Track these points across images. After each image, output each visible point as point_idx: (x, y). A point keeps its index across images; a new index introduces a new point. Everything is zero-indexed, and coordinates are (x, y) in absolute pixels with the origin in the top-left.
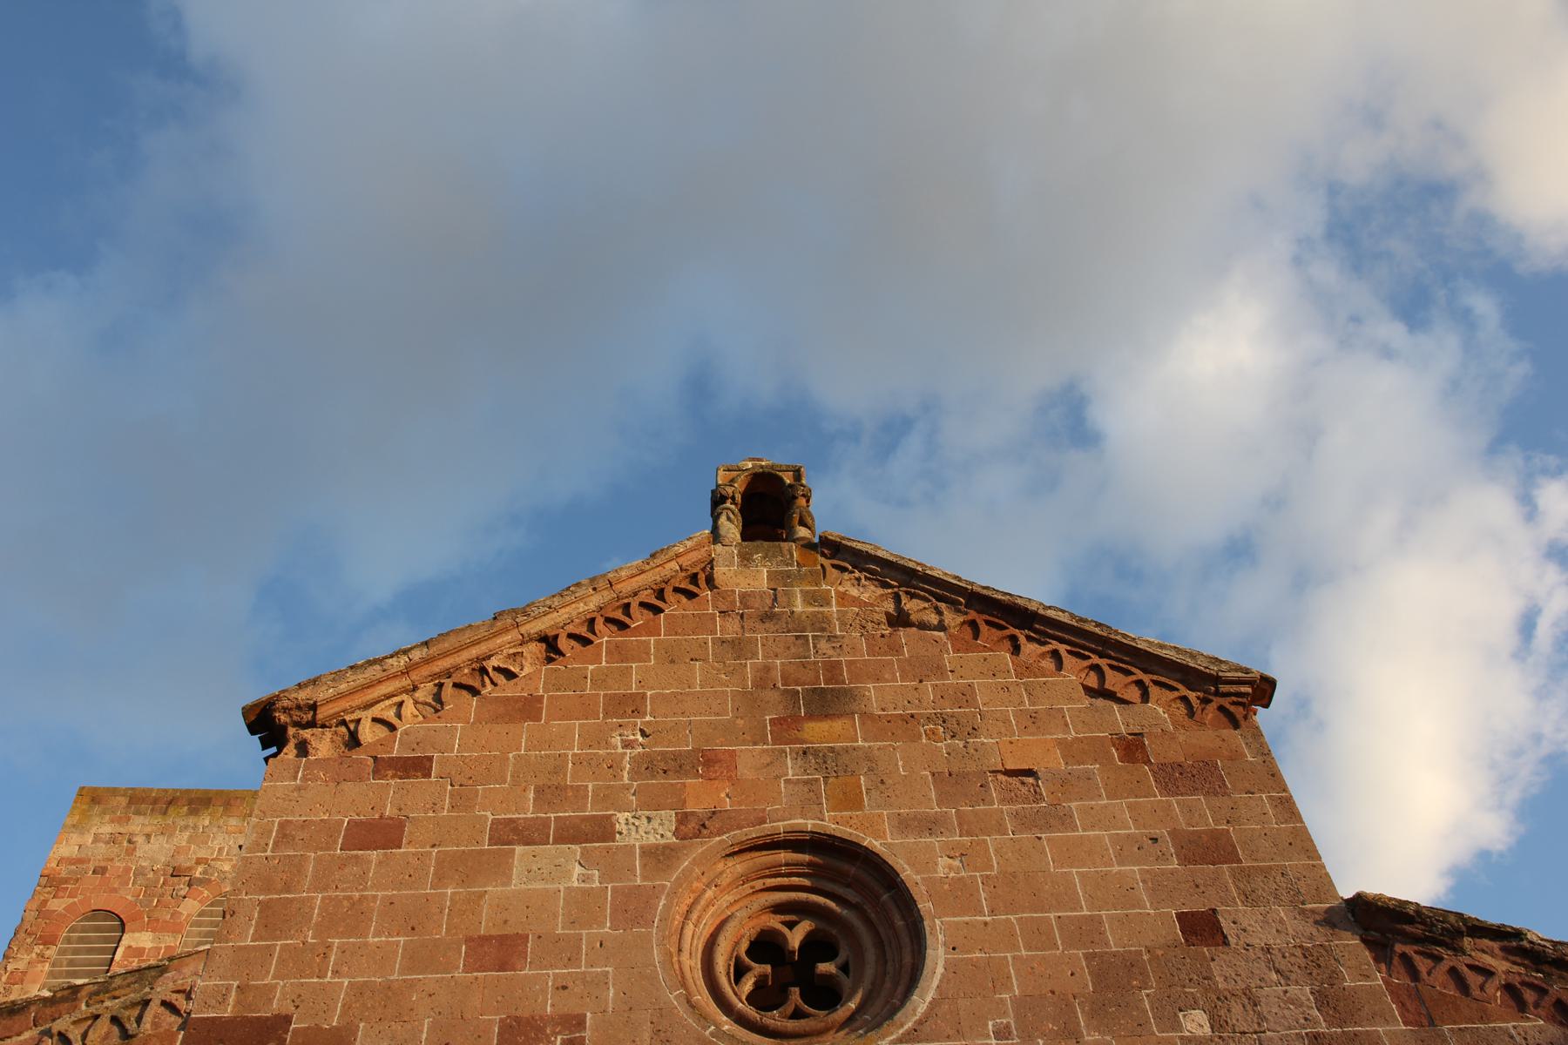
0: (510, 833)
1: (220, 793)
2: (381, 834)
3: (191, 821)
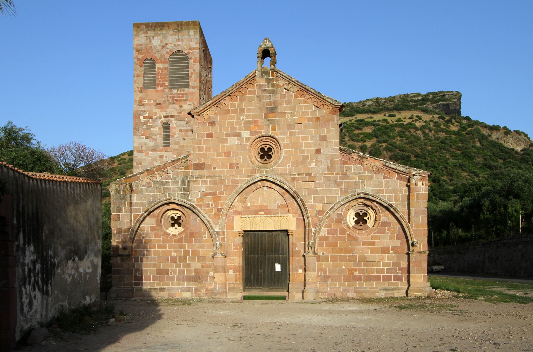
0: (228, 135)
1: (166, 23)
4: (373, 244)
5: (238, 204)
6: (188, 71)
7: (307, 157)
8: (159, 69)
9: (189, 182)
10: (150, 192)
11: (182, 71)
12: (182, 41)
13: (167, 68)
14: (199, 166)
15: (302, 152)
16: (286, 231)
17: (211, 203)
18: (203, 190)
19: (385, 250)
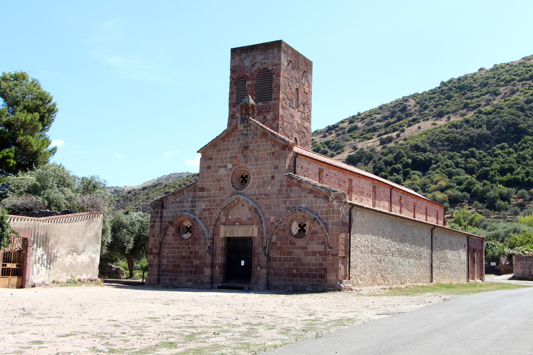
0: (220, 167)
2: (209, 167)
3: (252, 53)
4: (306, 248)
6: (272, 85)
7: (266, 181)
8: (248, 85)
9: (195, 201)
10: (173, 208)
11: (267, 86)
12: (268, 59)
13: (255, 84)
14: (202, 189)
15: (263, 178)
16: (251, 237)
17: (208, 216)
18: (203, 207)
19: (314, 253)
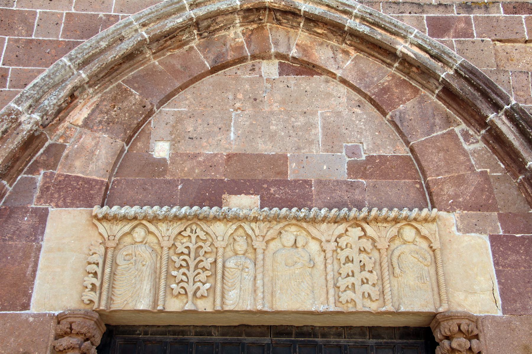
5: (88, 140)
